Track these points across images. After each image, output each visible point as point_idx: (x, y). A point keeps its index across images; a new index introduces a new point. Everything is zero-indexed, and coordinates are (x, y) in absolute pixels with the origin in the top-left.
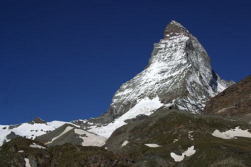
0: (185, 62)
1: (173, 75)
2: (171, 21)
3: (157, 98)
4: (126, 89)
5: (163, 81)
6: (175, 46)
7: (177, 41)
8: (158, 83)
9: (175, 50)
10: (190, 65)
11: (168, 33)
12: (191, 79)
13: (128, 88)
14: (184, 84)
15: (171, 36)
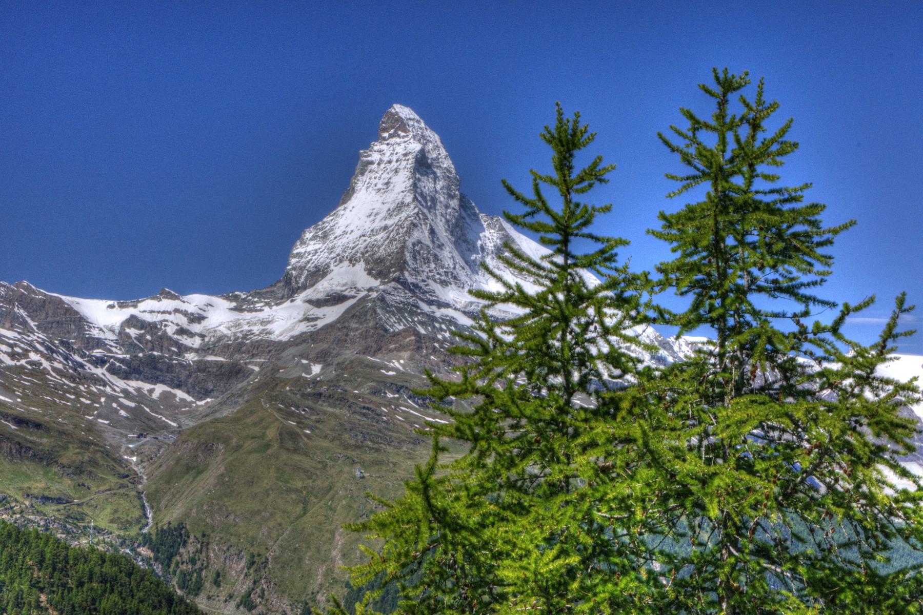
0: (409, 199)
1: (389, 222)
2: (391, 106)
3: (361, 265)
4: (311, 240)
5: (373, 232)
6: (397, 161)
7: (400, 150)
8: (364, 236)
9: (396, 171)
10: (416, 210)
11: (385, 130)
12: (416, 235)
13: (314, 238)
14: (403, 247)
15: (391, 136)
